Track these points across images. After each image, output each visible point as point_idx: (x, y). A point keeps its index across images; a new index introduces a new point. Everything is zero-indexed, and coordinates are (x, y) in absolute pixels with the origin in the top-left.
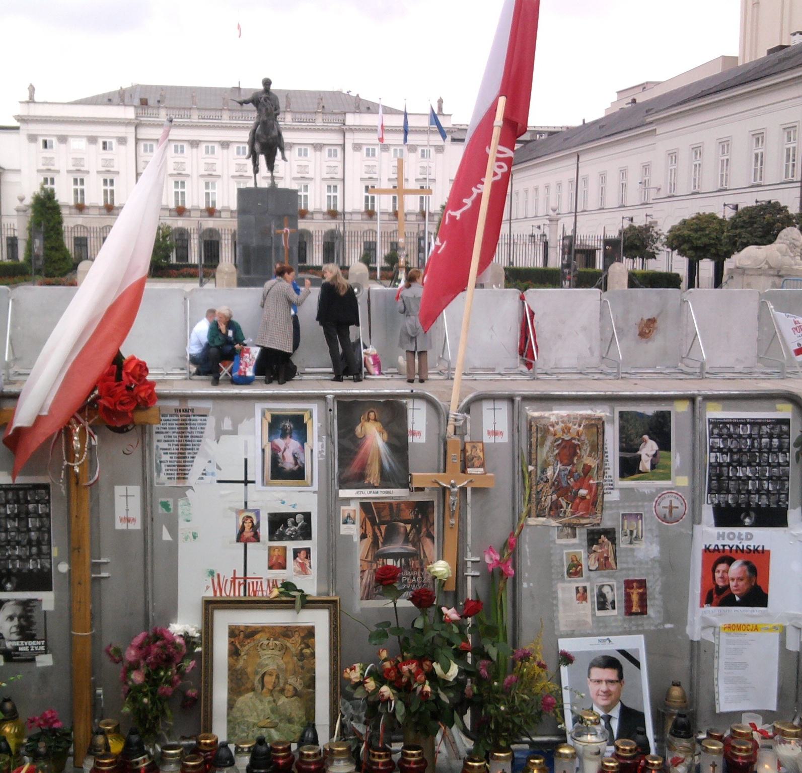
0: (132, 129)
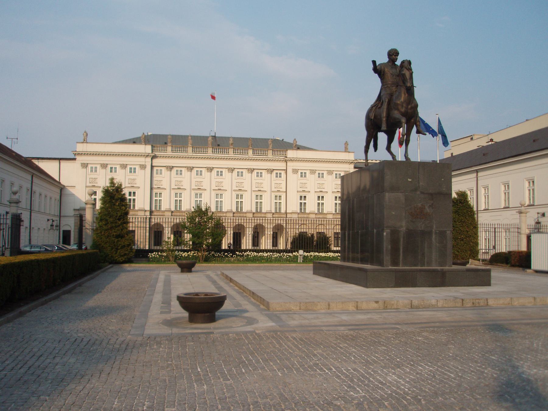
0: (149, 159)
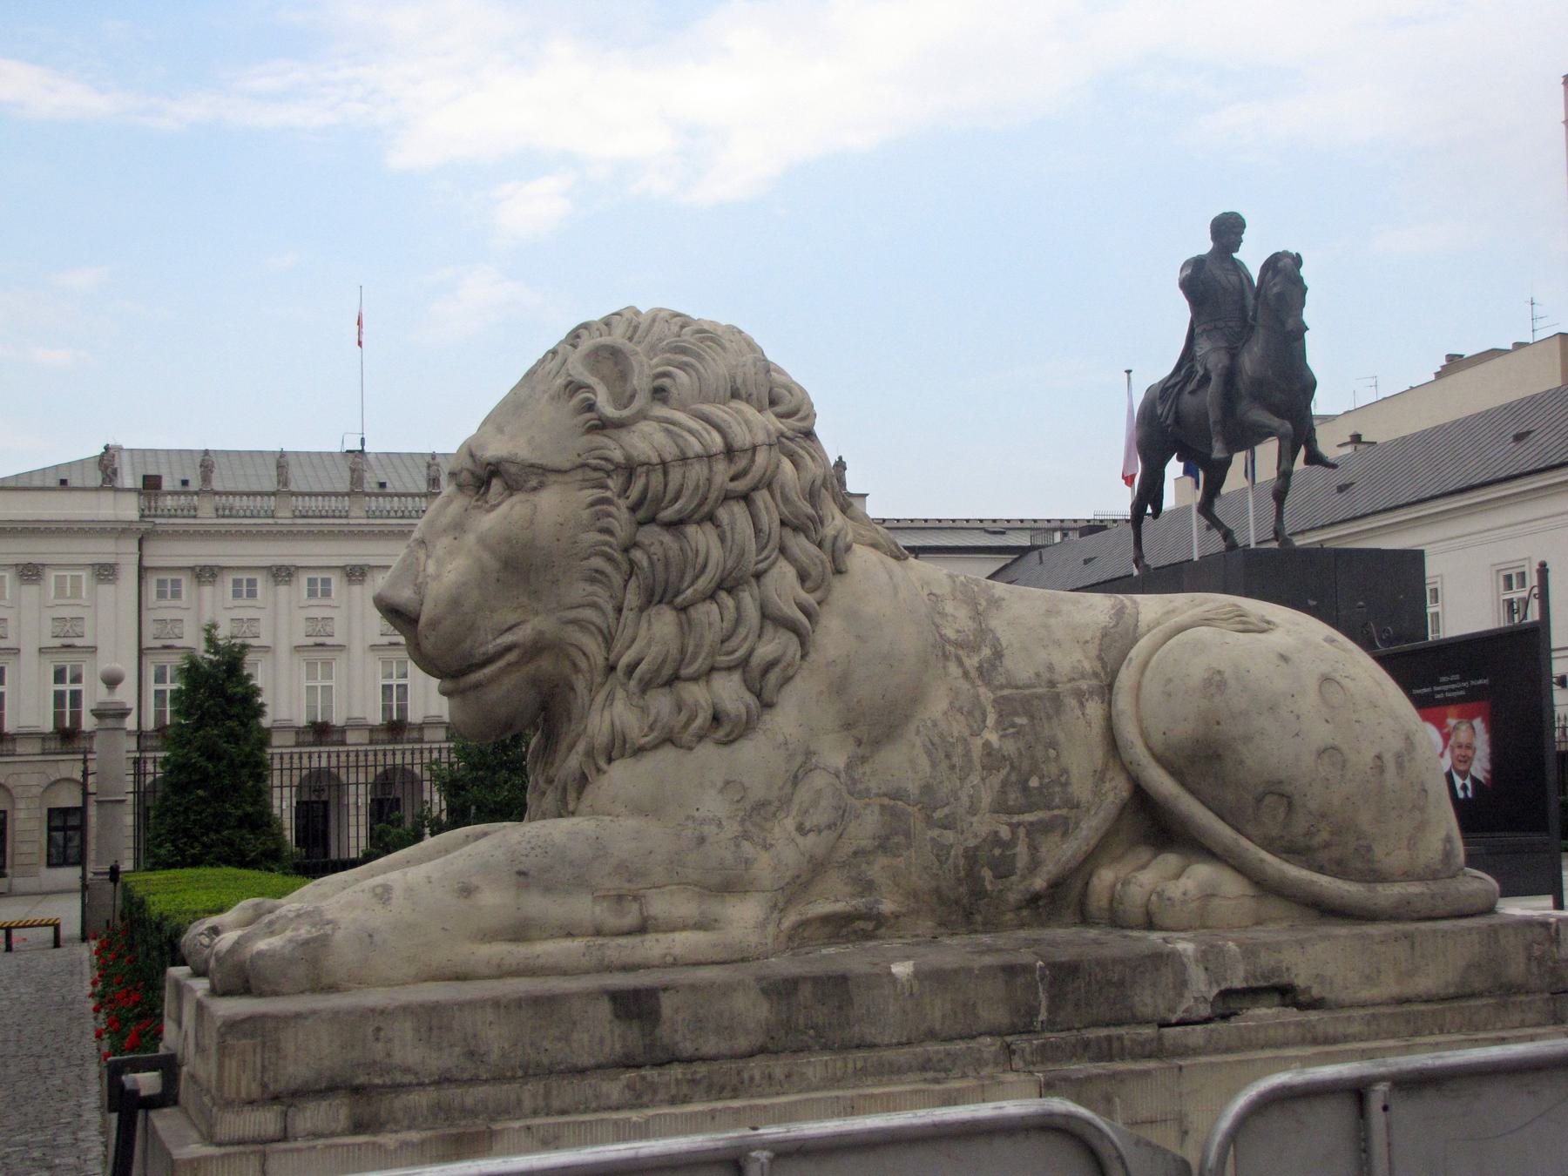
0: (132, 545)
